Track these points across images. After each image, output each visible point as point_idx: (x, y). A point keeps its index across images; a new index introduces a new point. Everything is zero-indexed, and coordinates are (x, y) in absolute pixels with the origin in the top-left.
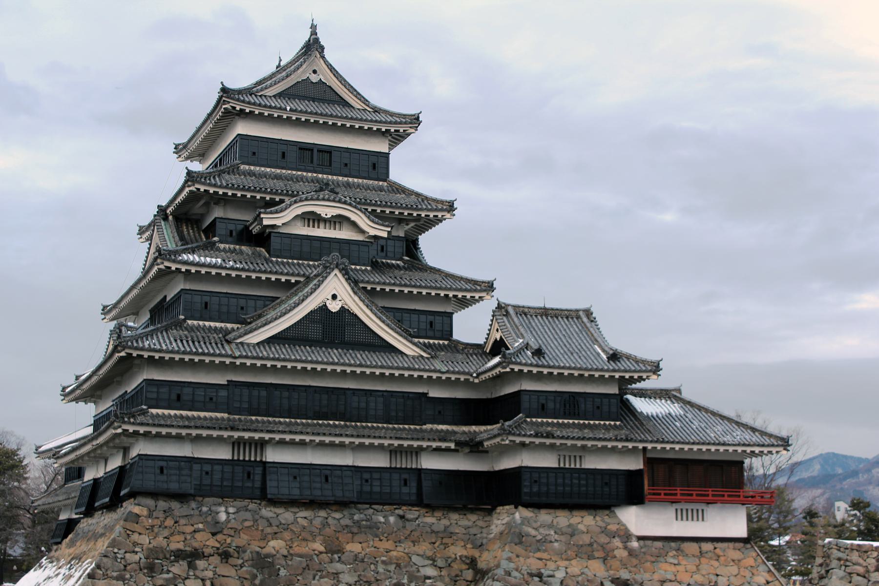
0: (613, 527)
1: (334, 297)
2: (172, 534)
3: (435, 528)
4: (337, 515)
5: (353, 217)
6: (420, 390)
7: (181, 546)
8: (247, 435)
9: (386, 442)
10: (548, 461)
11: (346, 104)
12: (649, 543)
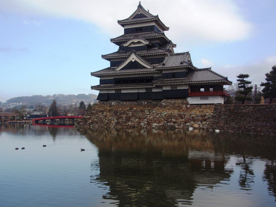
0: (185, 102)
1: (133, 59)
2: (102, 107)
3: (154, 104)
4: (135, 102)
5: (141, 41)
6: (152, 75)
7: (103, 110)
8: (118, 88)
9: (145, 87)
10: (169, 88)
11: (146, 17)
12: (193, 105)
